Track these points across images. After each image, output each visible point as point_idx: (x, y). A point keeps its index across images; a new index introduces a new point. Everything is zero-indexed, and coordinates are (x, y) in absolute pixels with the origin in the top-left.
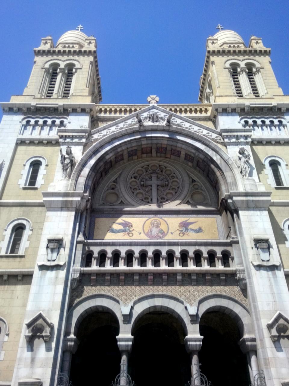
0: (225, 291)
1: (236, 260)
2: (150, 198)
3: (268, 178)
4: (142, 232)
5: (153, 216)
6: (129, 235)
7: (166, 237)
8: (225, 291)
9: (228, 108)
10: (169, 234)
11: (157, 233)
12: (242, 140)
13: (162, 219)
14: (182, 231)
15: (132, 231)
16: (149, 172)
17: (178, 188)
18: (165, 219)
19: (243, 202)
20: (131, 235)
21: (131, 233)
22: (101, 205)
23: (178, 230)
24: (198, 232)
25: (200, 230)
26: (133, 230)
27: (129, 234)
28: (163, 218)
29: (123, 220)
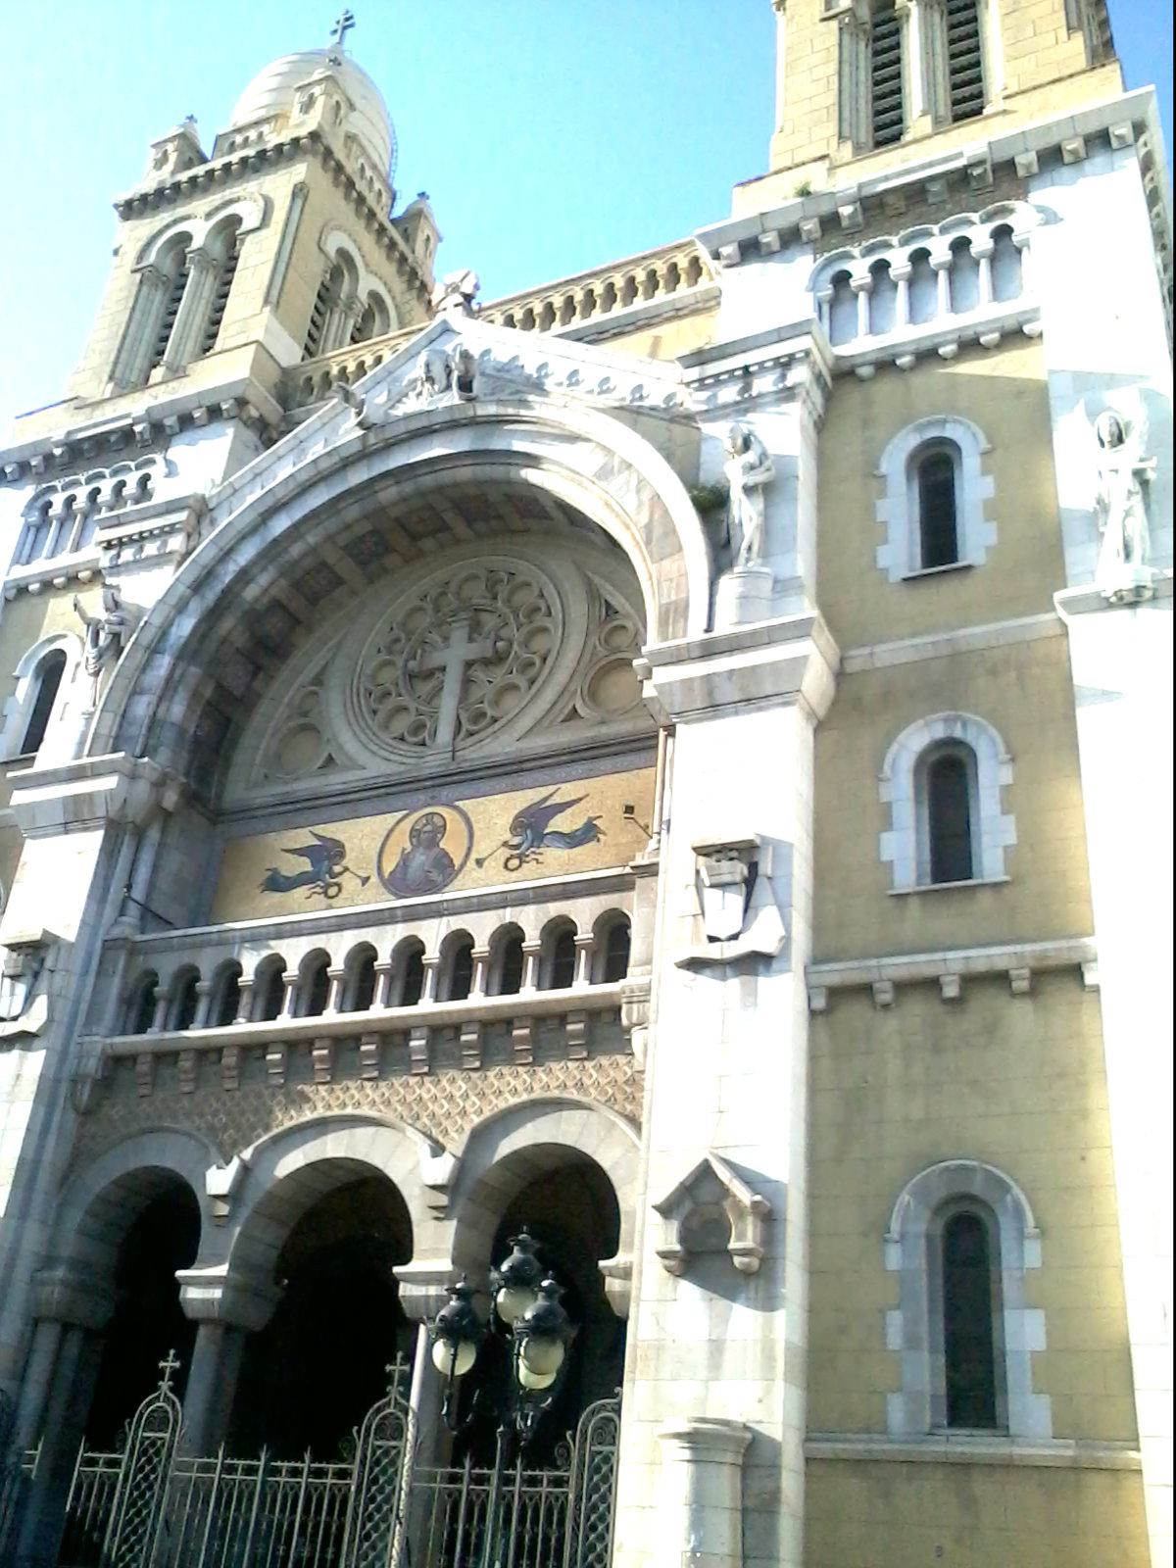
3: (885, 541)
4: (374, 879)
5: (421, 797)
6: (325, 893)
8: (580, 1086)
10: (471, 864)
11: (426, 868)
13: (456, 808)
15: (341, 874)
19: (691, 689)
20: (332, 891)
22: (257, 785)
23: (505, 844)
25: (588, 833)
26: (346, 869)
28: (457, 803)
29: (315, 835)
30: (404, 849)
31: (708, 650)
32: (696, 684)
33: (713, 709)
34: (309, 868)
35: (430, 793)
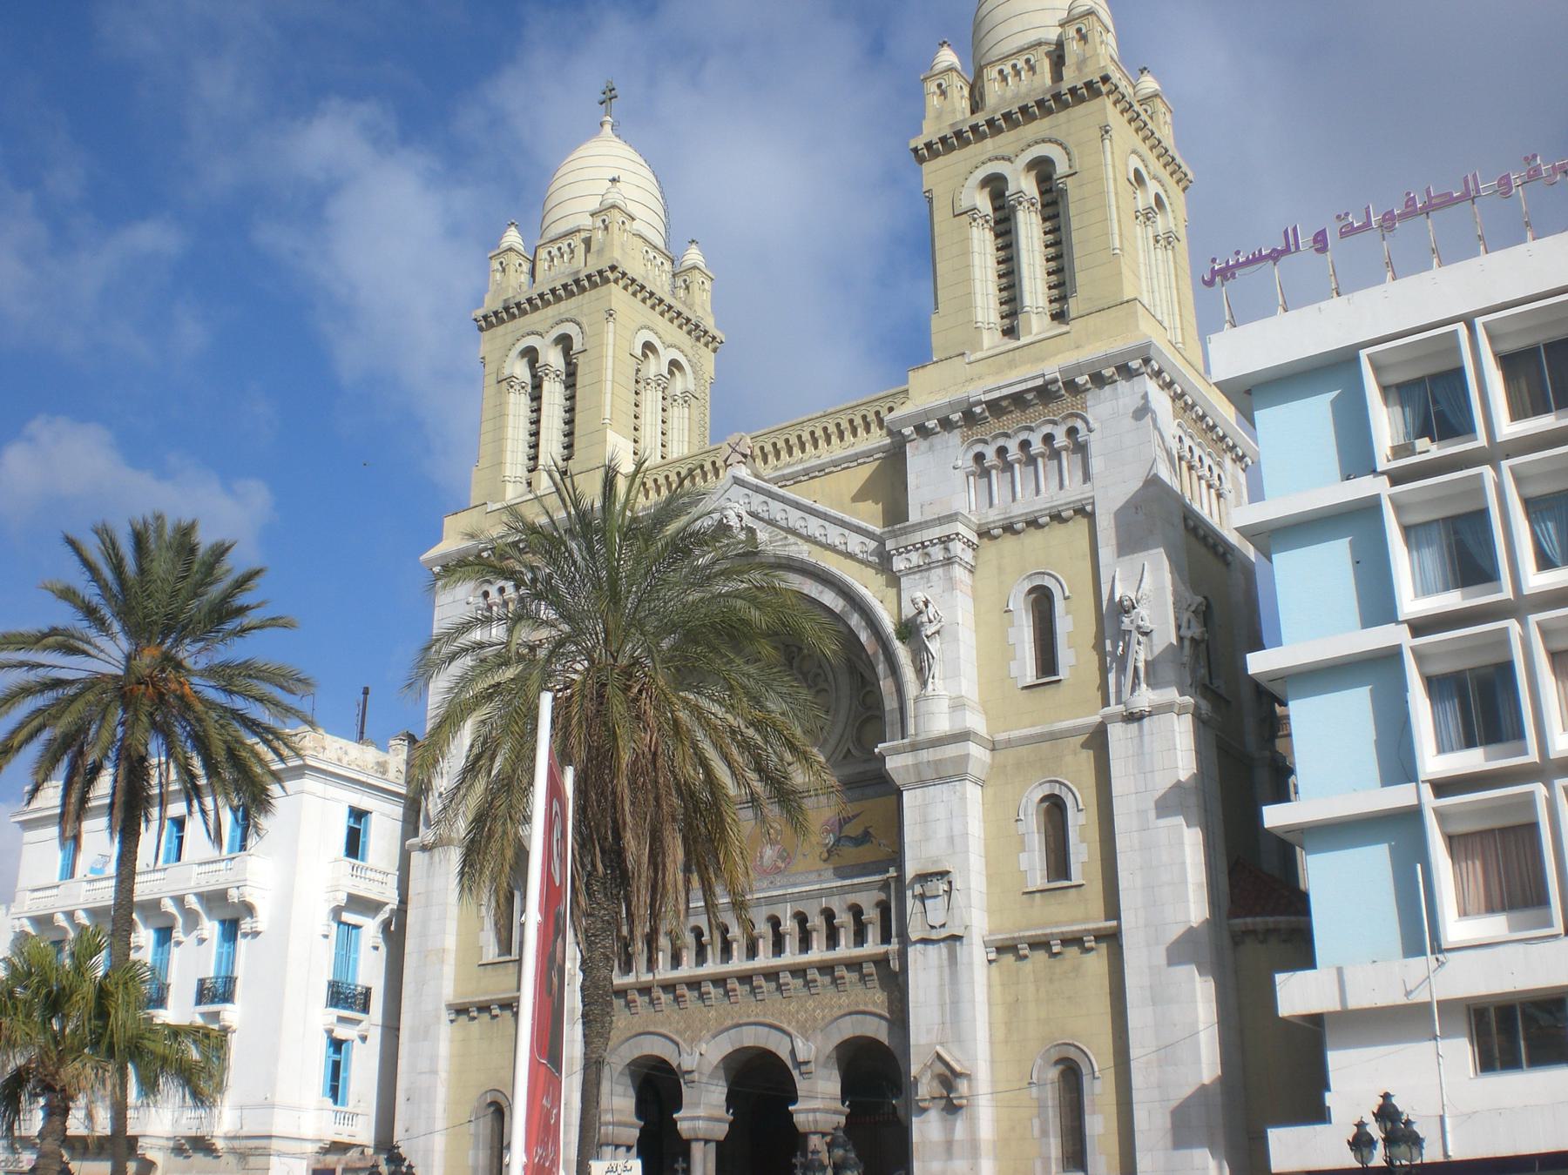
0: (874, 1003)
9: (928, 420)
12: (937, 553)
31: (915, 747)
32: (911, 770)
33: (922, 783)
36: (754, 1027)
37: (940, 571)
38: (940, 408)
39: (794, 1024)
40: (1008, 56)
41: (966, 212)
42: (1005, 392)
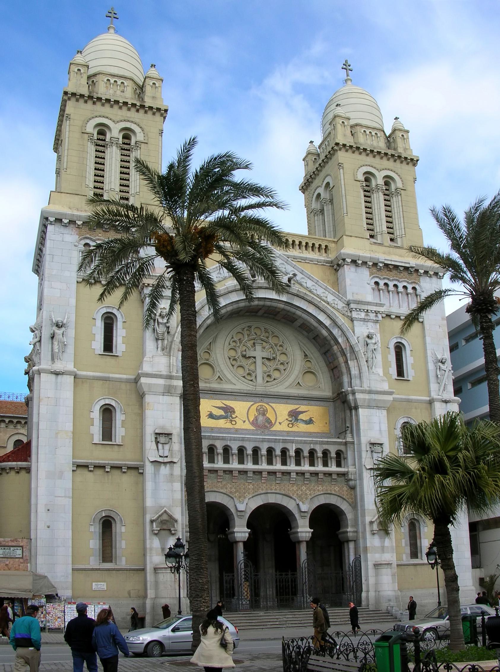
1: (350, 461)
2: (254, 375)
4: (247, 421)
5: (258, 399)
6: (231, 423)
7: (274, 429)
10: (277, 423)
13: (269, 405)
14: (291, 421)
16: (252, 337)
17: (287, 363)
18: (273, 405)
21: (234, 421)
23: (287, 419)
24: (309, 424)
25: (310, 422)
26: (237, 417)
27: (231, 421)
30: (255, 415)
34: (223, 414)
35: (262, 399)
36: (274, 494)
37: (372, 324)
38: (365, 257)
39: (295, 495)
40: (368, 127)
41: (360, 181)
42: (393, 263)
